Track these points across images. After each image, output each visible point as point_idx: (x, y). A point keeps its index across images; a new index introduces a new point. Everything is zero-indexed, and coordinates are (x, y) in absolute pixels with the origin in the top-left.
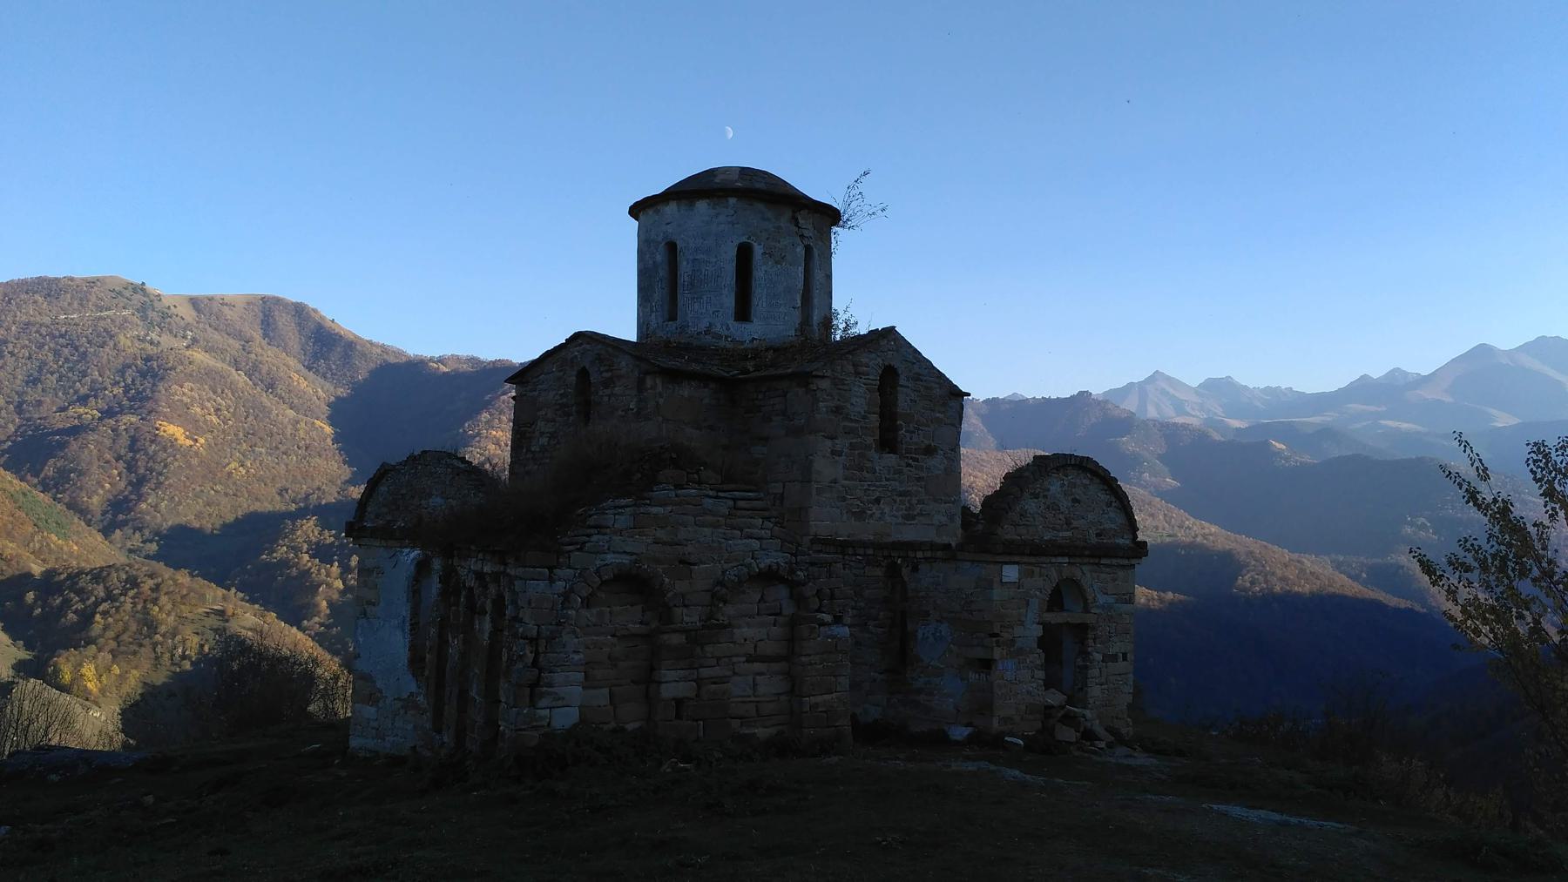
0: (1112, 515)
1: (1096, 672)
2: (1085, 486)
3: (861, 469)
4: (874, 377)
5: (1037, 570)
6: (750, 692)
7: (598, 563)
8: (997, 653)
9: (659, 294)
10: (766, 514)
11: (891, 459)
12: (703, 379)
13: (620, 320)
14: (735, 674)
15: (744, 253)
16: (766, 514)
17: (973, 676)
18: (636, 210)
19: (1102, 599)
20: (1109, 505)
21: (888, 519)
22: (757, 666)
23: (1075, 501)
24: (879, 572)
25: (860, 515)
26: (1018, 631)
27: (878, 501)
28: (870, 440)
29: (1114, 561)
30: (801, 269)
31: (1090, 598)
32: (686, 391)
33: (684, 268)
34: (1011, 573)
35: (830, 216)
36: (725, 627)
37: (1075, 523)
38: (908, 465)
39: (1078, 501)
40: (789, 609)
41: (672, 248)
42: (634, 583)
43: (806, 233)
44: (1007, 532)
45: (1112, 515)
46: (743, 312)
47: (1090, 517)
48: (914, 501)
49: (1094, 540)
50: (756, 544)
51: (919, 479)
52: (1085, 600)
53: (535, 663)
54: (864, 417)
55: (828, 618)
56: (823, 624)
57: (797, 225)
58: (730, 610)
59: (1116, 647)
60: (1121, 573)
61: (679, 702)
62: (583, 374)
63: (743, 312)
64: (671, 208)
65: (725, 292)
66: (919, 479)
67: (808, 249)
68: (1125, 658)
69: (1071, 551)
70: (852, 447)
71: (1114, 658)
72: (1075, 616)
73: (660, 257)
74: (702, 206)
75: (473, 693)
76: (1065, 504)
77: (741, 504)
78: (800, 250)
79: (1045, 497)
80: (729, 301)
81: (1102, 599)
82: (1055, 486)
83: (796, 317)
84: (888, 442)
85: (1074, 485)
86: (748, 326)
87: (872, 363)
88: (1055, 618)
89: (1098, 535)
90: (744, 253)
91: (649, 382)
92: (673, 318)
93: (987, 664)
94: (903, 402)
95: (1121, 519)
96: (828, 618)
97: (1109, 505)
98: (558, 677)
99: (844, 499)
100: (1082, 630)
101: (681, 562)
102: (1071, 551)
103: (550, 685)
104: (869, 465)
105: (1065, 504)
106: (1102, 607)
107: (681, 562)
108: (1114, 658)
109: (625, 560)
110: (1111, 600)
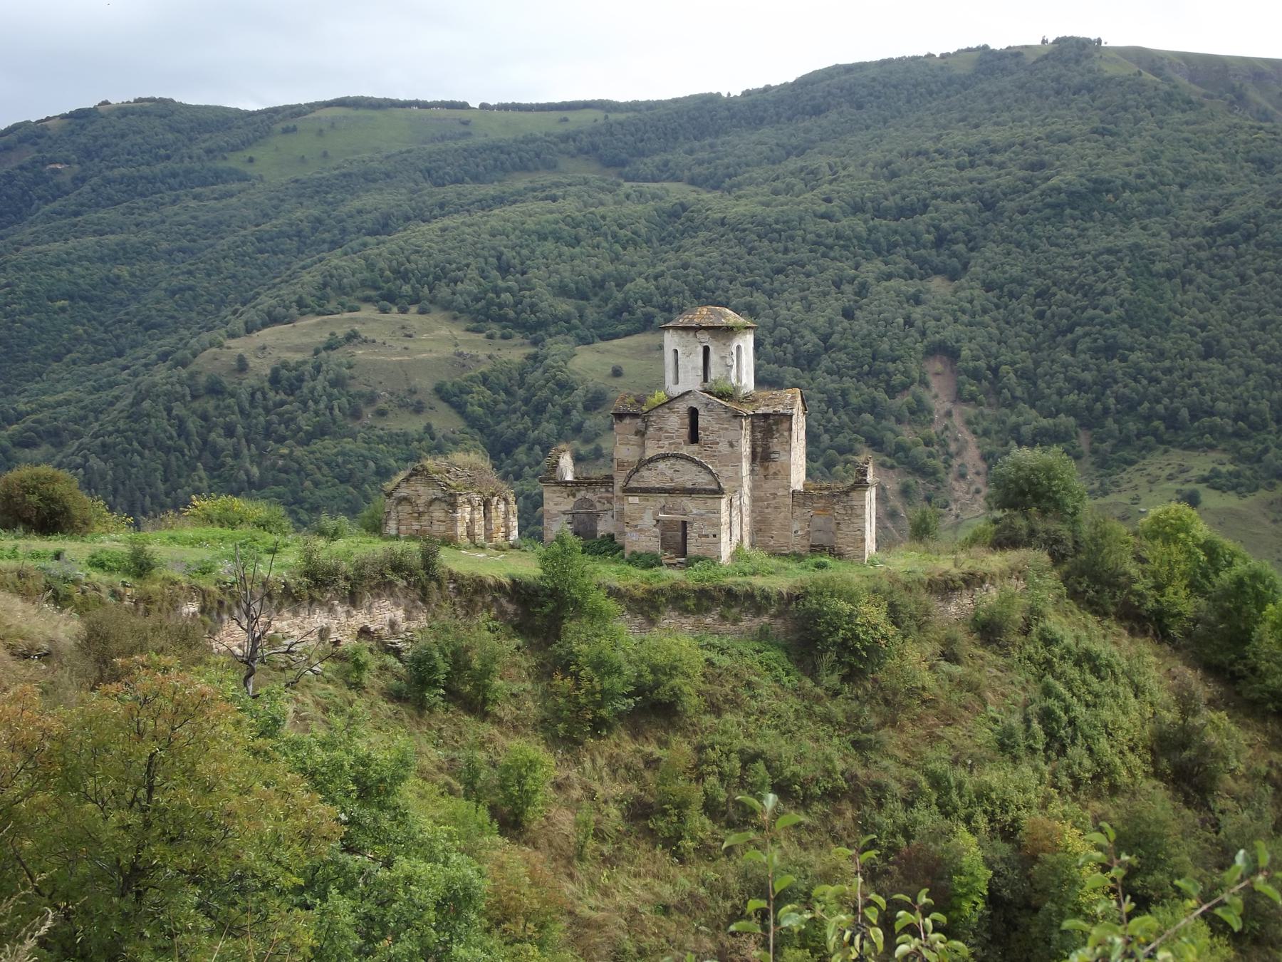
11: (695, 448)
19: (695, 511)
32: (627, 421)
34: (634, 500)
42: (406, 499)
44: (633, 484)
63: (677, 383)
67: (706, 350)
69: (670, 491)
71: (707, 536)
78: (700, 350)
81: (695, 511)
82: (662, 465)
83: (701, 379)
95: (710, 477)
102: (670, 491)
105: (669, 472)
108: (707, 536)
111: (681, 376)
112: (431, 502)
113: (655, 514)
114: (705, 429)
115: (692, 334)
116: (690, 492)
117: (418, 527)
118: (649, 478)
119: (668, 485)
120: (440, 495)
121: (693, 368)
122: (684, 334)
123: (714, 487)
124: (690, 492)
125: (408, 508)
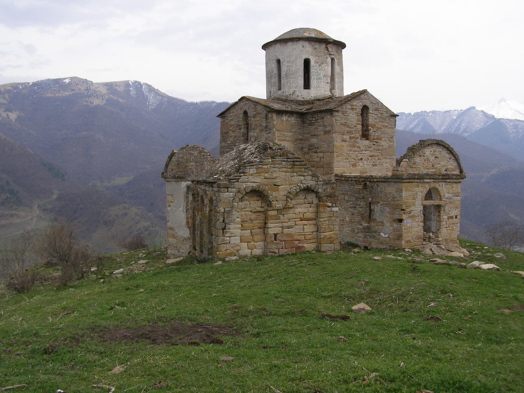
0: (451, 162)
1: (444, 223)
2: (440, 151)
3: (354, 147)
4: (359, 110)
5: (420, 185)
6: (302, 231)
7: (245, 186)
8: (404, 217)
9: (275, 80)
10: (306, 167)
11: (367, 142)
12: (291, 113)
13: (259, 91)
14: (296, 225)
15: (307, 63)
16: (306, 167)
17: (395, 225)
18: (265, 47)
19: (447, 195)
20: (450, 159)
21: (366, 166)
22: (304, 222)
23: (436, 157)
24: (361, 187)
25: (354, 165)
26: (413, 208)
27: (361, 159)
28: (358, 135)
29: (452, 181)
30: (330, 68)
31: (442, 195)
32: (284, 118)
33: (284, 69)
35: (341, 45)
36: (291, 208)
37: (436, 166)
38: (374, 145)
39: (437, 158)
40: (315, 201)
41: (279, 61)
42: (258, 193)
43: (331, 53)
45: (451, 162)
46: (307, 85)
47: (442, 163)
48: (377, 158)
49: (444, 173)
50: (302, 178)
51: (379, 150)
52: (440, 196)
53: (224, 221)
54: (355, 126)
55: (330, 204)
56: (329, 207)
57: (328, 50)
58: (294, 202)
59: (453, 213)
60: (455, 185)
61: (275, 235)
62: (245, 113)
63: (307, 85)
64: (278, 46)
65: (300, 78)
66: (379, 150)
67: (333, 60)
68: (456, 217)
70: (351, 138)
71: (452, 217)
72: (436, 202)
73: (274, 65)
74: (290, 44)
75: (205, 232)
76: (432, 158)
77: (297, 163)
78: (329, 60)
79: (424, 156)
80: (301, 82)
81: (447, 195)
82: (428, 151)
84: (365, 135)
85: (435, 151)
86: (307, 90)
87: (358, 104)
88: (428, 203)
89: (446, 170)
90: (307, 63)
91: (270, 116)
92: (280, 89)
93: (401, 221)
94: (371, 119)
95: (455, 164)
96: (330, 204)
97: (450, 159)
98: (232, 226)
99: (348, 159)
100: (438, 207)
101: (274, 185)
103: (229, 229)
104: (357, 145)
105: (432, 158)
106: (447, 198)
107: (274, 185)
108: (452, 217)
109: (255, 185)
110: (451, 195)
111: (313, 82)
112: (289, 196)
113: (422, 200)
114: (373, 126)
115: (323, 46)
116: (445, 178)
117: (277, 230)
118: (421, 164)
119: (432, 171)
120: (310, 182)
121: (324, 76)
122: (317, 46)
123: (457, 172)
124: (445, 178)
125: (256, 204)
